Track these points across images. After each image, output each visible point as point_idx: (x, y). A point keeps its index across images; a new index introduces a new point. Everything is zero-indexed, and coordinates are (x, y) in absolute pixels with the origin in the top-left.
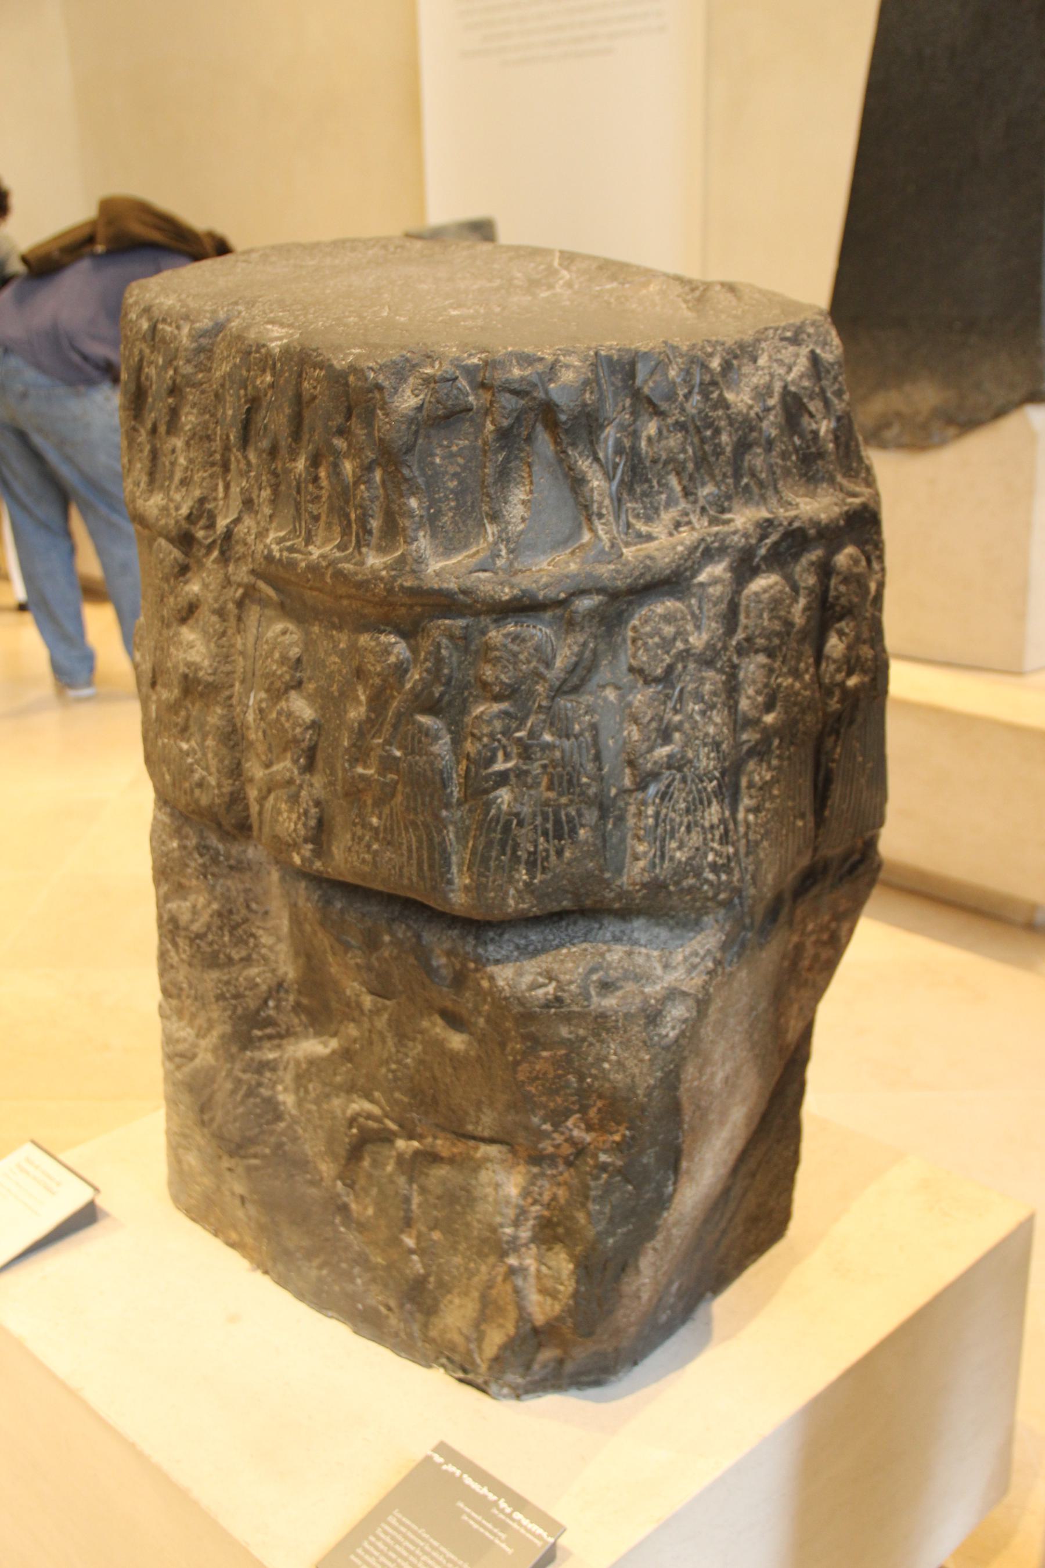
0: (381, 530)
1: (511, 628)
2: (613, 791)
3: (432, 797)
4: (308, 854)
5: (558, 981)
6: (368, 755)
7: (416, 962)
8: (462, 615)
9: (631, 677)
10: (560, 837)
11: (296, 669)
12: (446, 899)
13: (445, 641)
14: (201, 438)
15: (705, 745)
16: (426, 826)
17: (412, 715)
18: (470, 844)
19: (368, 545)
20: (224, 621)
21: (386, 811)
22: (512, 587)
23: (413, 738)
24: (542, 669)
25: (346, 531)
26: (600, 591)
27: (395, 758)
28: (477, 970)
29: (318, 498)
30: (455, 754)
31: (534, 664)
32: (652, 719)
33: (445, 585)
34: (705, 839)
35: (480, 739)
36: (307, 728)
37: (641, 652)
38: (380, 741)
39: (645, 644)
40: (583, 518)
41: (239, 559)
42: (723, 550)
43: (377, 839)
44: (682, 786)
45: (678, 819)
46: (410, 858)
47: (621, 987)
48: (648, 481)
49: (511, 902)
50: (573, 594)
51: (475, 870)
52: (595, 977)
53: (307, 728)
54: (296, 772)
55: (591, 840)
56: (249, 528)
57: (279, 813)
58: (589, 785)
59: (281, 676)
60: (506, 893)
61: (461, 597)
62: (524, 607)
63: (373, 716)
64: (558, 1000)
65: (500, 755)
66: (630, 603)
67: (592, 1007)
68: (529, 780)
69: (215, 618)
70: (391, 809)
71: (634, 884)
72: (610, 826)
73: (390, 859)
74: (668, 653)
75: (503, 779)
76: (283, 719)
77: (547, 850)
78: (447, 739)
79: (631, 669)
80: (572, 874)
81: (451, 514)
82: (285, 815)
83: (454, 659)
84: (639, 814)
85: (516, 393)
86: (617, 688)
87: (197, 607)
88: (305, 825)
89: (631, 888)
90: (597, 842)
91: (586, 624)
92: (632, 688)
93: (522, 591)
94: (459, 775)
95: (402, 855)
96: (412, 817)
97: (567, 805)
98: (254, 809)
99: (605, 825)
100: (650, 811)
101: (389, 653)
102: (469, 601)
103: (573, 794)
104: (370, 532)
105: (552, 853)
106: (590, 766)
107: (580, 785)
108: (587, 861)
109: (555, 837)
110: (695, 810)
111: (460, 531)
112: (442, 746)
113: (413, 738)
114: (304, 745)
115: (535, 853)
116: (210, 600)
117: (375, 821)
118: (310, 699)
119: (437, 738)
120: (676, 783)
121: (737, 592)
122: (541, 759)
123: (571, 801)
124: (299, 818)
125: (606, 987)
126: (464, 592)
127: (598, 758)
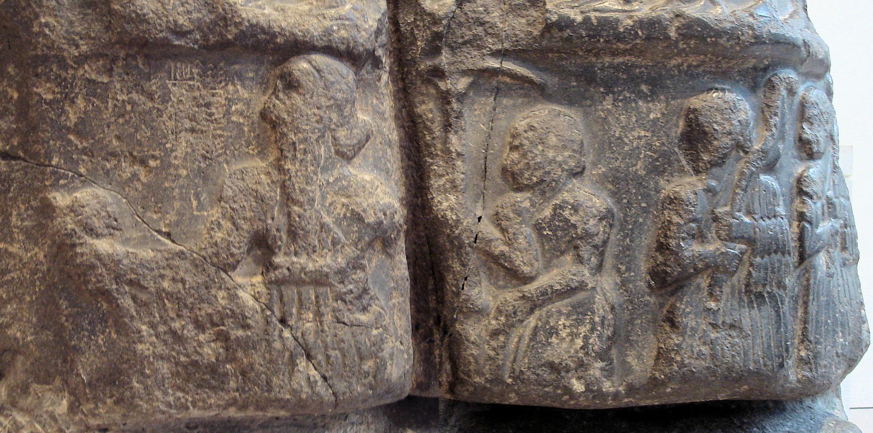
27: (746, 223)
53: (601, 219)
57: (553, 331)
114: (597, 240)
124: (593, 330)
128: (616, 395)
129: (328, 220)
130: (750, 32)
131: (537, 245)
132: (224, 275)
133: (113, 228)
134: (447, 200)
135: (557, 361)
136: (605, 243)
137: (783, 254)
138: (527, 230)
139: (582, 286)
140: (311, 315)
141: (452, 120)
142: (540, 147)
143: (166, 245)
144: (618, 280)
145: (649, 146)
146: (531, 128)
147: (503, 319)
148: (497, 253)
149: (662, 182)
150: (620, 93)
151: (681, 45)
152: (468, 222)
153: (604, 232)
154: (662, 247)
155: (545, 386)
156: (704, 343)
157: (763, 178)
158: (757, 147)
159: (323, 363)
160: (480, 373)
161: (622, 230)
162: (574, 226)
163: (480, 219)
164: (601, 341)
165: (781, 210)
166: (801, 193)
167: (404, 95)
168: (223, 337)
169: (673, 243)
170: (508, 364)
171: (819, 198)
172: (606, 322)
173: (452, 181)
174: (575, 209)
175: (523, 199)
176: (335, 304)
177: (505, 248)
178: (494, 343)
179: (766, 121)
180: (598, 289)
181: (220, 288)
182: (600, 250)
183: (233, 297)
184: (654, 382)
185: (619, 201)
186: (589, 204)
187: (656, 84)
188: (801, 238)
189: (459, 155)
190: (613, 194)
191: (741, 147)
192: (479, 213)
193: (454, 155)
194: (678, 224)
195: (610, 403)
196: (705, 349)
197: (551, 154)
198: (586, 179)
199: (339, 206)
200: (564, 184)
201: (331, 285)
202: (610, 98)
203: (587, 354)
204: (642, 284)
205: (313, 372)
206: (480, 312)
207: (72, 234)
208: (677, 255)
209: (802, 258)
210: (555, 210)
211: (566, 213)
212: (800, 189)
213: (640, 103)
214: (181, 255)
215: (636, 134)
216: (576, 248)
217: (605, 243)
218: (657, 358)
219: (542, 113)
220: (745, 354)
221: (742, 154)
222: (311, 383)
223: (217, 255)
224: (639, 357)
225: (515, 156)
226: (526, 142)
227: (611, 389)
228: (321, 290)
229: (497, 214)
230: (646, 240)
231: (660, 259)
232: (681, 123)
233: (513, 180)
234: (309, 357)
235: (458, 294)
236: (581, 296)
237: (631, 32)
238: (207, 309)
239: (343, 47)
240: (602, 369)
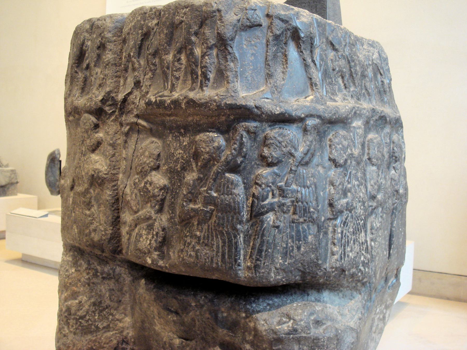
0: (215, 79)
1: (277, 130)
2: (323, 219)
3: (233, 217)
4: (156, 257)
5: (294, 320)
6: (197, 197)
7: (209, 316)
8: (255, 120)
9: (329, 163)
10: (299, 240)
11: (157, 160)
12: (236, 275)
13: (245, 134)
14: (112, 65)
15: (359, 201)
16: (228, 233)
17: (224, 174)
18: (251, 244)
19: (207, 86)
20: (115, 149)
21: (205, 227)
22: (281, 107)
23: (224, 186)
24: (293, 151)
25: (194, 81)
26: (319, 117)
27: (213, 197)
28: (247, 317)
29: (180, 69)
30: (246, 195)
31: (289, 148)
32: (340, 184)
33: (248, 104)
34: (360, 248)
35: (260, 186)
36: (161, 190)
37: (334, 151)
38: (205, 189)
39: (336, 147)
40: (309, 84)
41: (129, 112)
42: (360, 115)
43: (199, 243)
44: (351, 220)
45: (350, 236)
46: (218, 252)
47: (325, 324)
48: (331, 78)
49: (273, 275)
50: (307, 116)
51: (254, 257)
52: (312, 318)
53: (161, 190)
54: (153, 212)
55: (314, 242)
56: (136, 96)
57: (141, 236)
58: (314, 212)
59: (149, 163)
60: (270, 270)
61: (256, 110)
62: (284, 120)
63: (202, 176)
64: (295, 331)
65: (270, 194)
66: (328, 128)
67: (311, 334)
68: (285, 208)
69: (109, 148)
70: (209, 226)
71: (332, 268)
72: (321, 237)
73: (206, 254)
74: (345, 153)
75: (271, 208)
76: (148, 186)
77: (292, 247)
78: (242, 186)
79: (330, 159)
80: (304, 260)
81: (250, 72)
82: (144, 237)
83: (249, 144)
84: (334, 231)
85: (282, 20)
86: (324, 168)
87: (101, 144)
88: (156, 241)
89: (330, 270)
90: (316, 243)
91: (313, 132)
92: (330, 169)
93: (285, 110)
94: (247, 206)
95: (214, 250)
96: (221, 229)
97: (302, 223)
98: (124, 239)
99: (319, 235)
100: (339, 230)
101: (214, 142)
102: (259, 113)
103: (306, 217)
104: (208, 80)
105: (295, 248)
106: (314, 203)
107: (309, 212)
108: (311, 254)
109: (296, 240)
110: (356, 233)
111: (254, 80)
112: (240, 191)
113: (224, 186)
114: (158, 198)
115: (286, 248)
116: (108, 139)
117: (198, 233)
118: (164, 174)
119: (237, 185)
120: (349, 218)
121: (365, 137)
122: (291, 197)
123: (305, 220)
124: (153, 237)
125: (318, 323)
126: (257, 107)
127: (317, 200)
135: (141, 248)
136: (163, 200)
150: (174, 133)
153: (162, 195)
156: (193, 251)
157: (227, 175)
161: (171, 195)
164: (156, 243)
172: (159, 235)
190: (170, 179)
196: (193, 254)
198: (160, 171)
213: (181, 138)
215: (178, 152)
221: (216, 163)
240: (158, 255)
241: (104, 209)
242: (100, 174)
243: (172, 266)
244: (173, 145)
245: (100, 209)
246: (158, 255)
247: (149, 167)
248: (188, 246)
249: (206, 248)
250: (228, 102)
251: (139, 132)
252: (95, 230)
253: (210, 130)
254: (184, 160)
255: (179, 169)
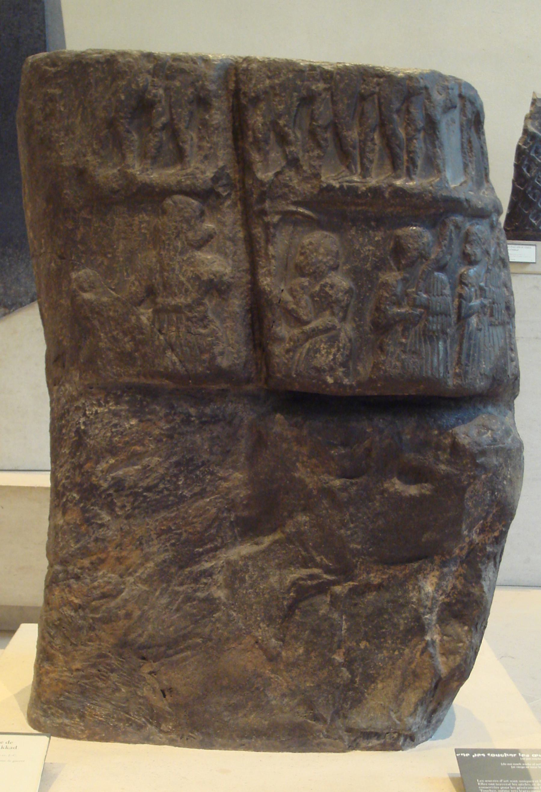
4: (341, 374)
19: (415, 174)
43: (404, 352)
54: (337, 321)
57: (318, 351)
59: (327, 262)
63: (408, 275)
95: (422, 358)
114: (343, 304)
124: (339, 350)
128: (351, 386)
129: (183, 279)
130: (430, 195)
131: (310, 305)
132: (134, 308)
133: (92, 287)
134: (266, 280)
136: (348, 306)
137: (446, 316)
138: (306, 297)
139: (334, 328)
140: (174, 329)
141: (270, 238)
142: (315, 254)
143: (111, 294)
144: (354, 326)
145: (374, 255)
146: (311, 243)
147: (292, 343)
148: (290, 308)
149: (380, 274)
151: (392, 202)
152: (276, 292)
153: (347, 300)
154: (378, 309)
155: (313, 379)
156: (398, 361)
158: (433, 257)
159: (180, 353)
160: (280, 372)
162: (331, 296)
163: (282, 290)
165: (447, 291)
166: (462, 283)
167: (247, 224)
168: (133, 339)
169: (383, 306)
170: (294, 367)
171: (473, 286)
173: (269, 271)
174: (332, 287)
175: (305, 281)
176: (186, 323)
177: (294, 306)
178: (287, 356)
179: (440, 243)
180: (343, 330)
181: (133, 315)
182: (345, 309)
183: (138, 319)
184: (371, 380)
185: (356, 284)
186: (340, 285)
187: (380, 221)
188: (460, 307)
189: (273, 257)
190: (354, 280)
191: (423, 257)
192: (282, 287)
193: (270, 257)
194: (386, 297)
195: (349, 393)
196: (398, 364)
197: (320, 258)
199: (189, 272)
200: (327, 274)
201: (184, 313)
202: (354, 228)
203: (335, 363)
204: (367, 328)
205: (174, 358)
206: (281, 340)
207: (75, 291)
208: (384, 312)
209: (460, 318)
210: (321, 287)
211: (327, 289)
212: (462, 282)
213: (370, 232)
214: (118, 299)
215: (367, 248)
216: (332, 307)
217: (348, 306)
218: (373, 368)
219: (317, 237)
220: (421, 368)
221: (424, 261)
222: (174, 364)
223: (132, 298)
224: (364, 367)
225: (302, 258)
226: (308, 251)
227: (348, 383)
228: (179, 315)
229: (291, 288)
230: (371, 305)
231: (377, 315)
232: (392, 243)
233: (300, 271)
234: (173, 350)
235: (270, 330)
236: (333, 333)
237: (365, 194)
238: (127, 325)
239: (188, 190)
240: (344, 372)
241: (233, 324)
242: (225, 278)
243: (360, 384)
244: (358, 240)
245: (225, 325)
246: (344, 372)
247: (327, 266)
248: (391, 357)
249: (415, 356)
250: (443, 194)
251: (295, 224)
252: (222, 354)
253: (414, 223)
254: (377, 258)
255: (369, 269)
